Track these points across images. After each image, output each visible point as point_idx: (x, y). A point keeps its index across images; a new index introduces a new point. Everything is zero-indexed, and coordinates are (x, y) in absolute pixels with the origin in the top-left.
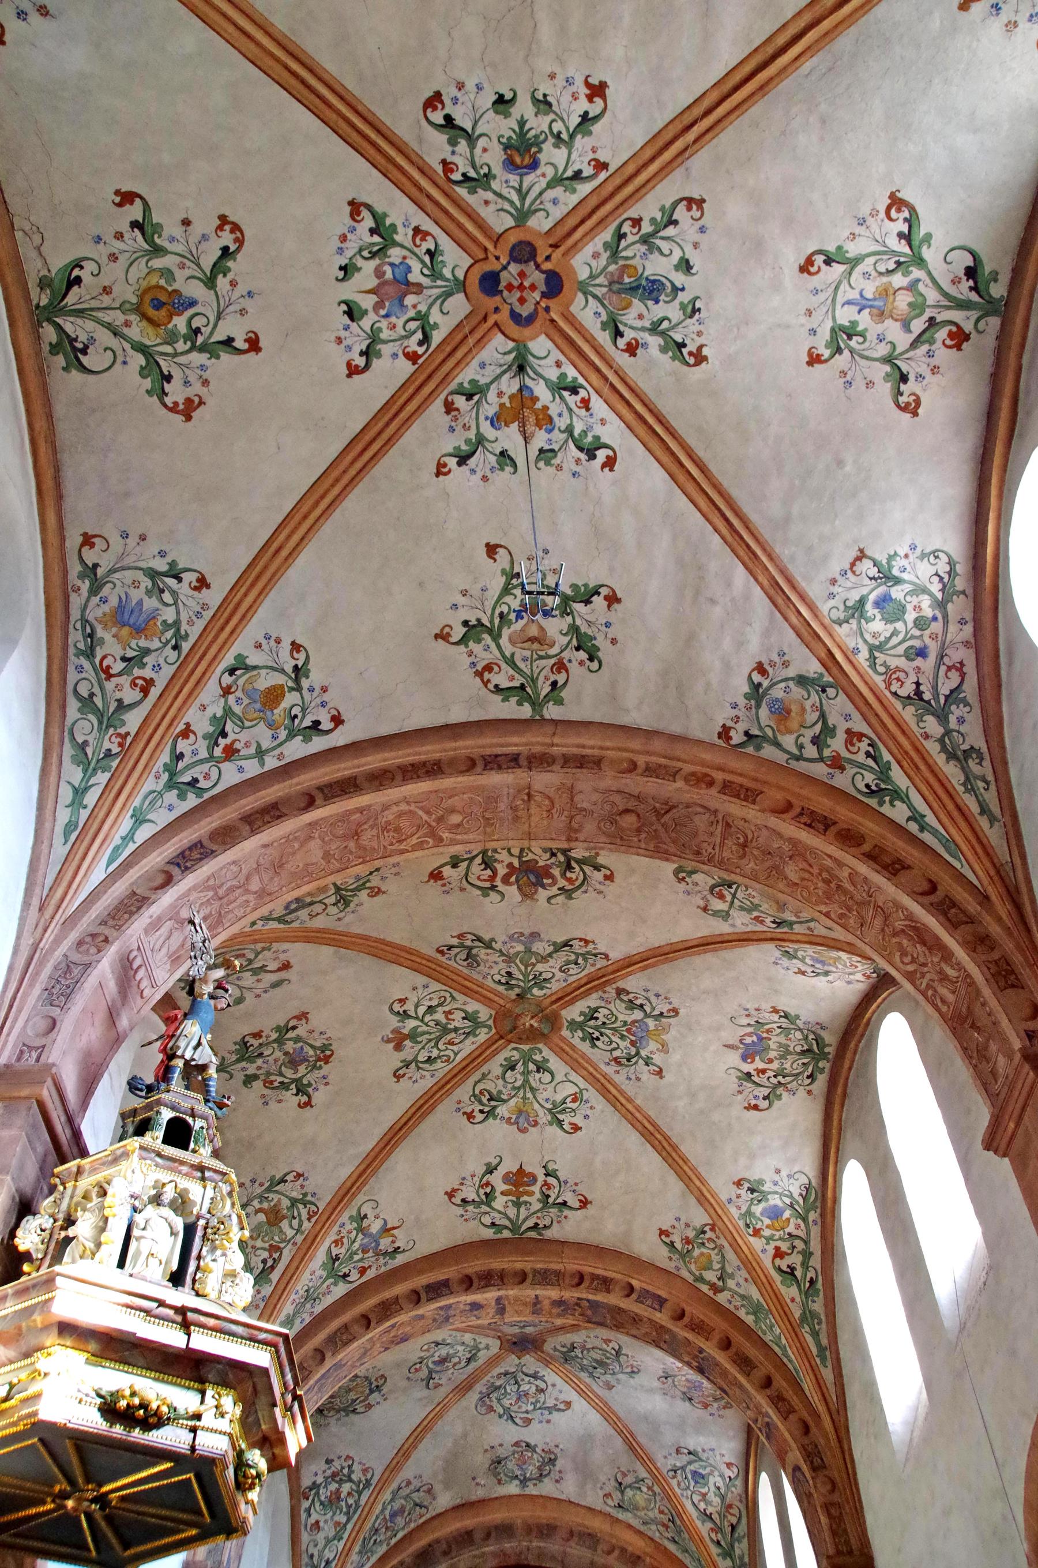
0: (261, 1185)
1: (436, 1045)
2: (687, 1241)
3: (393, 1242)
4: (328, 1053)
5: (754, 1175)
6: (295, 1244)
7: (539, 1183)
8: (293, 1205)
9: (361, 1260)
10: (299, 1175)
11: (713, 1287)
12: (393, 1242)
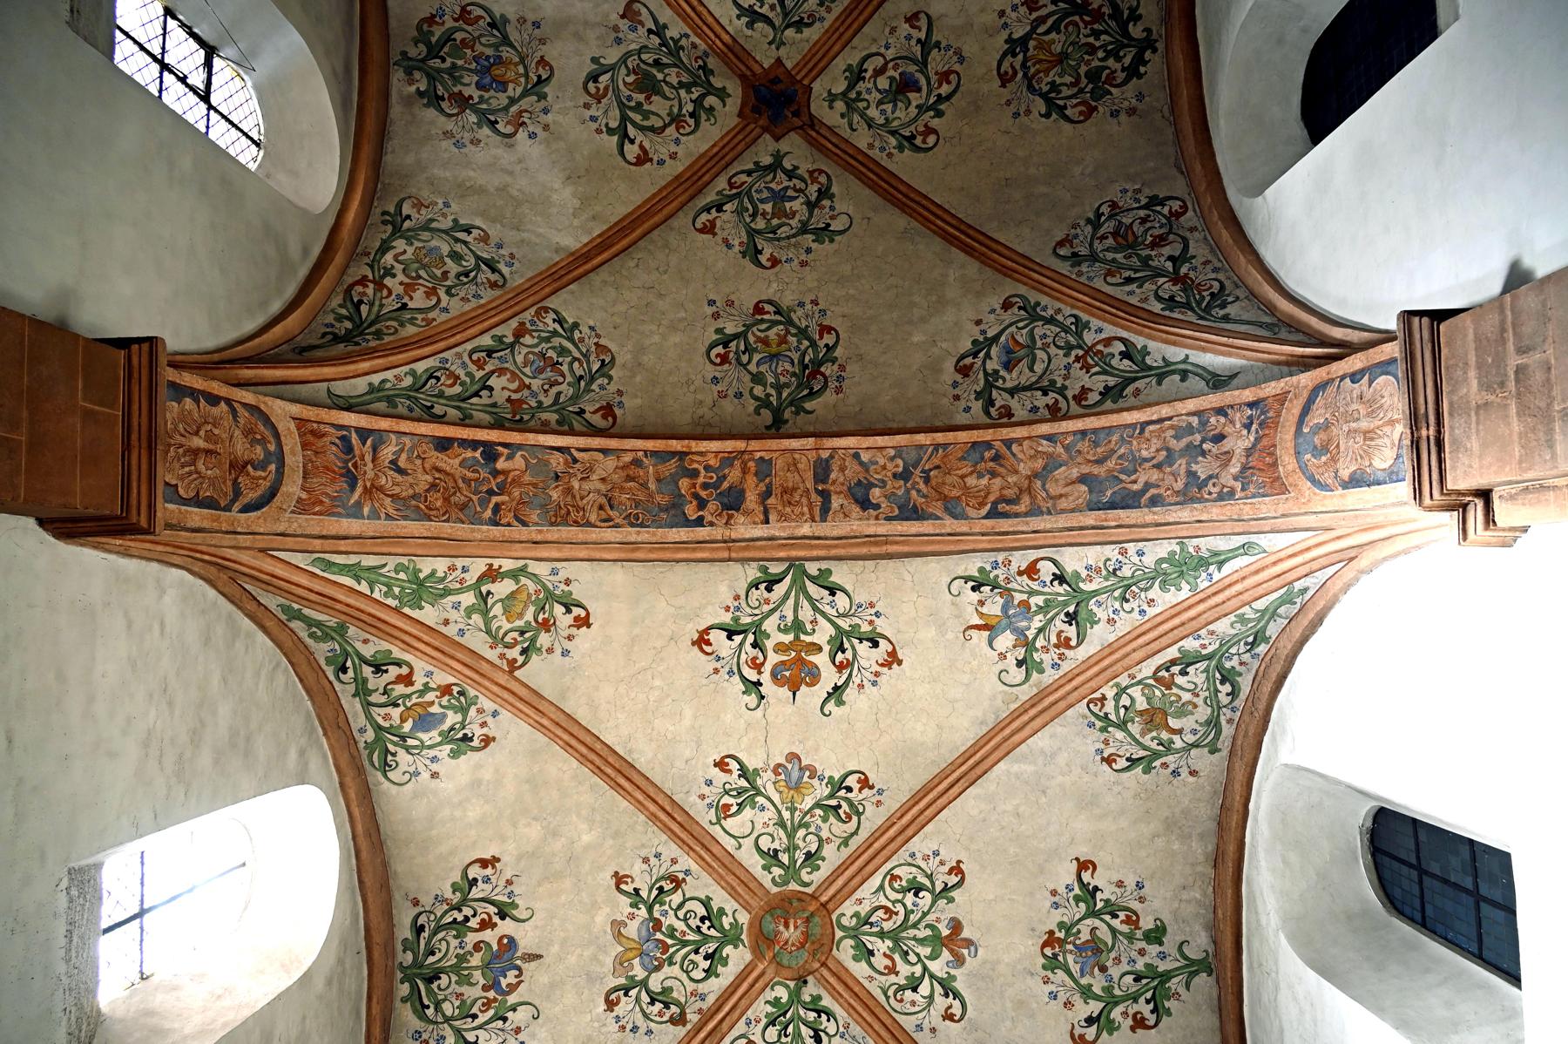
0: (1165, 766)
1: (908, 913)
2: (546, 626)
3: (982, 603)
4: (1048, 952)
5: (469, 759)
6: (1132, 677)
7: (768, 668)
8: (1125, 723)
9: (1032, 593)
10: (1109, 761)
11: (492, 575)
12: (982, 603)
